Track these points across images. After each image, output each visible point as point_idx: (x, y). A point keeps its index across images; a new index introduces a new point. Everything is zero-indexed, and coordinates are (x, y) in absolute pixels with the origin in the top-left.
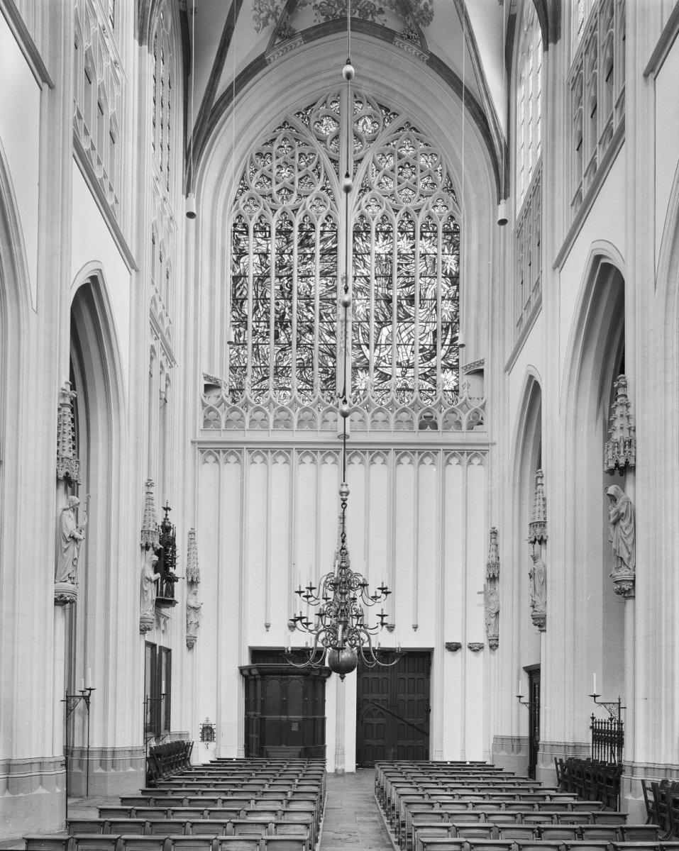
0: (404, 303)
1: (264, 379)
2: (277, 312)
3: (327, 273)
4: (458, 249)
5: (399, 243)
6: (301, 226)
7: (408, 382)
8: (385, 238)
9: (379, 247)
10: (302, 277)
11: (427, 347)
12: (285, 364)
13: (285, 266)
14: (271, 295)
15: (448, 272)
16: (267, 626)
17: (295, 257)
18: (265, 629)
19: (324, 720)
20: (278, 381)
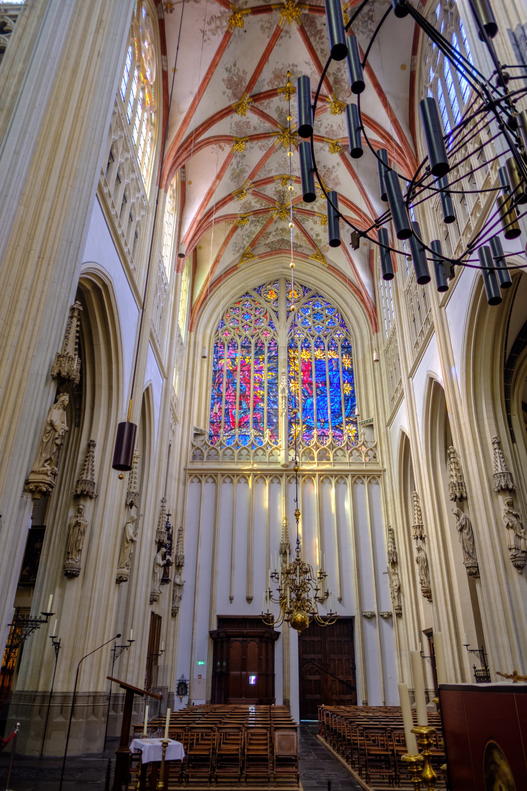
0: (320, 385)
1: (232, 429)
2: (241, 390)
3: (272, 369)
4: (351, 356)
5: (315, 353)
6: (256, 344)
7: (325, 431)
8: (306, 351)
9: (305, 355)
10: (257, 371)
11: (336, 410)
12: (246, 420)
13: (247, 365)
14: (238, 381)
15: (346, 368)
16: (231, 599)
17: (252, 361)
18: (229, 601)
19: (273, 675)
20: (241, 431)
